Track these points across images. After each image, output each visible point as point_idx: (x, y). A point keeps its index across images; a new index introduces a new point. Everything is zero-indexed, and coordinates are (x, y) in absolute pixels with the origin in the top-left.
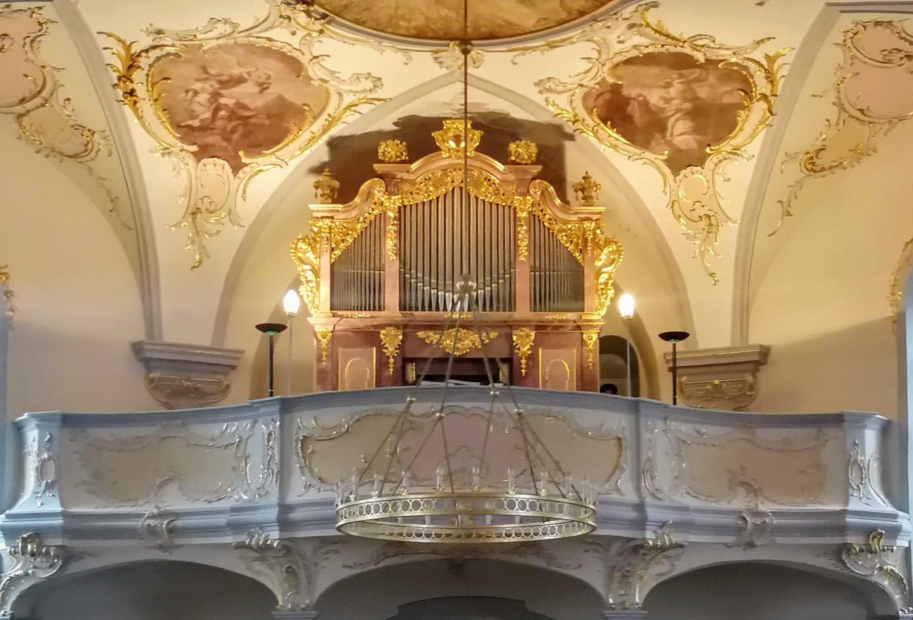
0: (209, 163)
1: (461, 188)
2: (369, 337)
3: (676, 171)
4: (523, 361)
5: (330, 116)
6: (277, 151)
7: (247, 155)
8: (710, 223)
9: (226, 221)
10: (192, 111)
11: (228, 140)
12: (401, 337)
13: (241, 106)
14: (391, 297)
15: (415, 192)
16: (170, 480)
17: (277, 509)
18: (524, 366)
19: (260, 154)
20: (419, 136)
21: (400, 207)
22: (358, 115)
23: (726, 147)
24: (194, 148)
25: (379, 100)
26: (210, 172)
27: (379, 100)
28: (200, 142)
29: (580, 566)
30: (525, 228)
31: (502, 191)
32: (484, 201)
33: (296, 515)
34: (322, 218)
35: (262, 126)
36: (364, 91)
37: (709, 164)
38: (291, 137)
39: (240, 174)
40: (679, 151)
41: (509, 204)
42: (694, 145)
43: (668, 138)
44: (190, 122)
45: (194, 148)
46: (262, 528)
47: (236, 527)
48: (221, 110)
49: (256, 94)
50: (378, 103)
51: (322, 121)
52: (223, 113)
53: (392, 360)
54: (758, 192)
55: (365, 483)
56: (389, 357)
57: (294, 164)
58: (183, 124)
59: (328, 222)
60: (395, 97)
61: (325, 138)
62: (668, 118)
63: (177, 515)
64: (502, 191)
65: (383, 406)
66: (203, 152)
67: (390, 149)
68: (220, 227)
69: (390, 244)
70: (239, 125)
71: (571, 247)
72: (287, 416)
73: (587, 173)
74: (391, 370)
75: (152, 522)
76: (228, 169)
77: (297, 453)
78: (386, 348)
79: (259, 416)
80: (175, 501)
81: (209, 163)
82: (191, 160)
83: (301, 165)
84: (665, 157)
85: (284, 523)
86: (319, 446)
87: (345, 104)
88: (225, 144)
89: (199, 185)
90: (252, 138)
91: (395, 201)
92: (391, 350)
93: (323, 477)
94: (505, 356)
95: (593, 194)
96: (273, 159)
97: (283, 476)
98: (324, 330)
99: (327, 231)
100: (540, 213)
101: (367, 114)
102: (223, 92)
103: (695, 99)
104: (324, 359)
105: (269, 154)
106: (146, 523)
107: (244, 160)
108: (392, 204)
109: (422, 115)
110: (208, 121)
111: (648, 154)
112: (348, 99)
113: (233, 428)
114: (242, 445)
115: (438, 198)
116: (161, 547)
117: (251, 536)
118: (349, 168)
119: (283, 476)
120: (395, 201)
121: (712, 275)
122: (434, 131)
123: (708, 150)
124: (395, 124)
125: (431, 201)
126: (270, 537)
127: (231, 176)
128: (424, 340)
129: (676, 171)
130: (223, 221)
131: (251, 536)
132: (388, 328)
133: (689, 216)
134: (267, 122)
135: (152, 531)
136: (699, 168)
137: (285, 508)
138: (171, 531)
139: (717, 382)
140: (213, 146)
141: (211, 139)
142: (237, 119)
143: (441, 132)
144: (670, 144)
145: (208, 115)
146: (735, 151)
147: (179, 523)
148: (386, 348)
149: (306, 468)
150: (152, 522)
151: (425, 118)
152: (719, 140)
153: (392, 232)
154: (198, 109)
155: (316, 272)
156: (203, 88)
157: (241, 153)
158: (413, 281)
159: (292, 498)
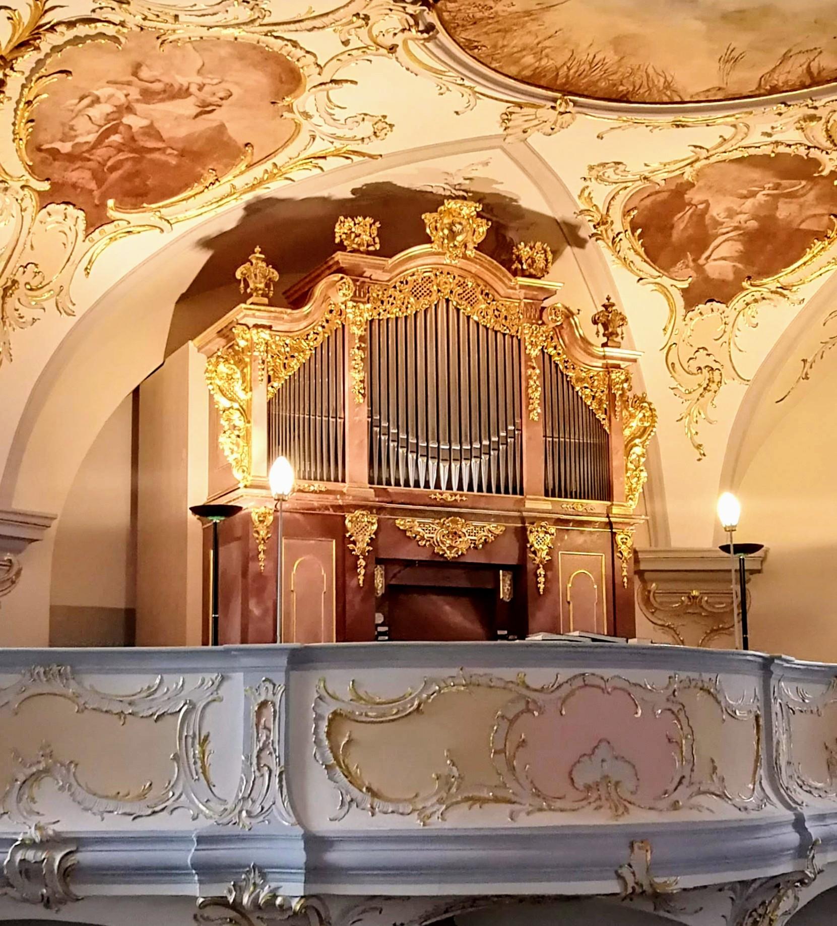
0: (57, 212)
1: (448, 301)
2: (329, 523)
3: (690, 304)
4: (541, 571)
5: (275, 165)
6: (163, 207)
7: (118, 207)
8: (711, 378)
9: (50, 305)
10: (72, 128)
11: (100, 182)
12: (375, 527)
13: (151, 131)
14: (357, 465)
15: (385, 299)
16: (47, 771)
17: (302, 844)
18: (541, 579)
19: (136, 206)
20: (399, 215)
21: (372, 321)
22: (319, 171)
23: (771, 283)
24: (45, 186)
25: (363, 154)
26: (48, 228)
27: (363, 154)
28: (56, 177)
29: (701, 909)
30: (538, 371)
31: (504, 313)
32: (478, 324)
33: (334, 857)
34: (256, 326)
35: (164, 165)
36: (354, 139)
37: (738, 302)
38: (197, 188)
39: (96, 235)
40: (707, 279)
41: (513, 333)
42: (730, 277)
43: (702, 261)
44: (57, 145)
45: (45, 186)
46: (263, 875)
47: (208, 871)
48: (116, 133)
49: (188, 118)
50: (356, 158)
51: (258, 172)
52: (116, 138)
53: (362, 562)
54: (787, 344)
55: (457, 803)
56: (357, 558)
57: (179, 229)
58: (45, 147)
59: (265, 335)
60: (389, 155)
61: (249, 197)
62: (716, 236)
63: (80, 842)
64: (504, 313)
65: (481, 671)
66: (58, 194)
67: (359, 230)
68: (37, 313)
69: (354, 378)
70: (127, 159)
71: (594, 406)
72: (294, 674)
73: (608, 299)
74: (361, 578)
75: (30, 855)
76: (82, 225)
77: (318, 742)
78: (354, 543)
79: (234, 670)
80: (63, 814)
81: (57, 212)
82: (31, 203)
83: (192, 231)
84: (685, 285)
85: (315, 871)
86: (360, 732)
87: (311, 151)
88: (93, 185)
89: (29, 244)
90: (137, 181)
91: (366, 311)
92: (362, 544)
93: (375, 788)
94: (513, 560)
95: (619, 330)
96: (153, 218)
97: (291, 779)
98: (262, 510)
99: (263, 348)
100: (554, 352)
101: (332, 171)
102: (139, 107)
103: (772, 218)
104: (261, 556)
105: (152, 210)
106: (19, 857)
107: (112, 214)
108: (357, 317)
109: (399, 184)
110: (85, 148)
111: (666, 281)
112: (318, 147)
113: (181, 685)
114: (195, 717)
115: (415, 315)
116: (47, 902)
117: (238, 888)
118: (290, 249)
119: (291, 779)
120: (366, 311)
121: (699, 447)
122: (424, 213)
123: (745, 284)
124: (354, 191)
125: (406, 317)
126: (280, 892)
127: (81, 235)
128: (405, 531)
129: (690, 304)
130: (45, 304)
131: (238, 888)
132: (358, 513)
133: (685, 365)
134: (173, 161)
135: (28, 870)
136: (724, 306)
137: (315, 843)
138: (67, 873)
139: (695, 593)
140: (74, 186)
141: (80, 176)
142: (133, 151)
143: (434, 214)
144: (700, 269)
145: (92, 138)
146: (782, 291)
147: (85, 857)
148: (354, 543)
149: (338, 765)
150: (30, 855)
151: (404, 188)
152: (768, 271)
153: (358, 358)
154: (81, 124)
155: (244, 412)
156: (111, 96)
157: (111, 203)
158: (383, 437)
159: (323, 825)
